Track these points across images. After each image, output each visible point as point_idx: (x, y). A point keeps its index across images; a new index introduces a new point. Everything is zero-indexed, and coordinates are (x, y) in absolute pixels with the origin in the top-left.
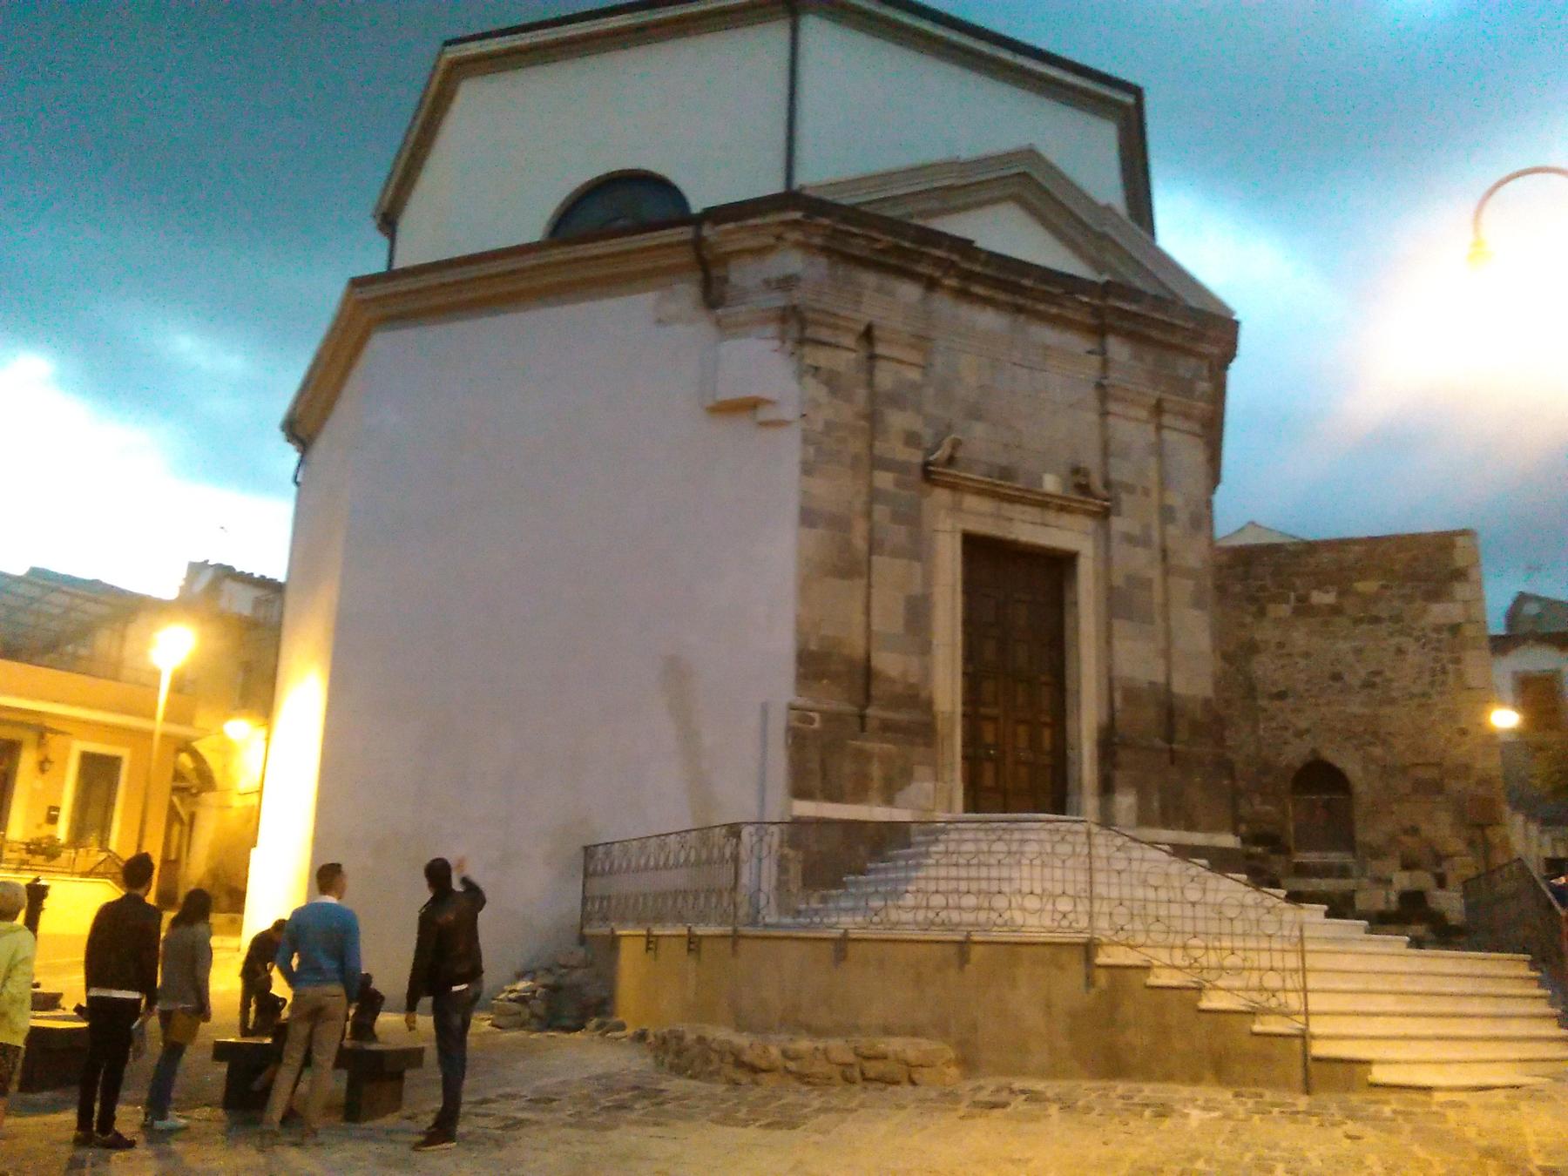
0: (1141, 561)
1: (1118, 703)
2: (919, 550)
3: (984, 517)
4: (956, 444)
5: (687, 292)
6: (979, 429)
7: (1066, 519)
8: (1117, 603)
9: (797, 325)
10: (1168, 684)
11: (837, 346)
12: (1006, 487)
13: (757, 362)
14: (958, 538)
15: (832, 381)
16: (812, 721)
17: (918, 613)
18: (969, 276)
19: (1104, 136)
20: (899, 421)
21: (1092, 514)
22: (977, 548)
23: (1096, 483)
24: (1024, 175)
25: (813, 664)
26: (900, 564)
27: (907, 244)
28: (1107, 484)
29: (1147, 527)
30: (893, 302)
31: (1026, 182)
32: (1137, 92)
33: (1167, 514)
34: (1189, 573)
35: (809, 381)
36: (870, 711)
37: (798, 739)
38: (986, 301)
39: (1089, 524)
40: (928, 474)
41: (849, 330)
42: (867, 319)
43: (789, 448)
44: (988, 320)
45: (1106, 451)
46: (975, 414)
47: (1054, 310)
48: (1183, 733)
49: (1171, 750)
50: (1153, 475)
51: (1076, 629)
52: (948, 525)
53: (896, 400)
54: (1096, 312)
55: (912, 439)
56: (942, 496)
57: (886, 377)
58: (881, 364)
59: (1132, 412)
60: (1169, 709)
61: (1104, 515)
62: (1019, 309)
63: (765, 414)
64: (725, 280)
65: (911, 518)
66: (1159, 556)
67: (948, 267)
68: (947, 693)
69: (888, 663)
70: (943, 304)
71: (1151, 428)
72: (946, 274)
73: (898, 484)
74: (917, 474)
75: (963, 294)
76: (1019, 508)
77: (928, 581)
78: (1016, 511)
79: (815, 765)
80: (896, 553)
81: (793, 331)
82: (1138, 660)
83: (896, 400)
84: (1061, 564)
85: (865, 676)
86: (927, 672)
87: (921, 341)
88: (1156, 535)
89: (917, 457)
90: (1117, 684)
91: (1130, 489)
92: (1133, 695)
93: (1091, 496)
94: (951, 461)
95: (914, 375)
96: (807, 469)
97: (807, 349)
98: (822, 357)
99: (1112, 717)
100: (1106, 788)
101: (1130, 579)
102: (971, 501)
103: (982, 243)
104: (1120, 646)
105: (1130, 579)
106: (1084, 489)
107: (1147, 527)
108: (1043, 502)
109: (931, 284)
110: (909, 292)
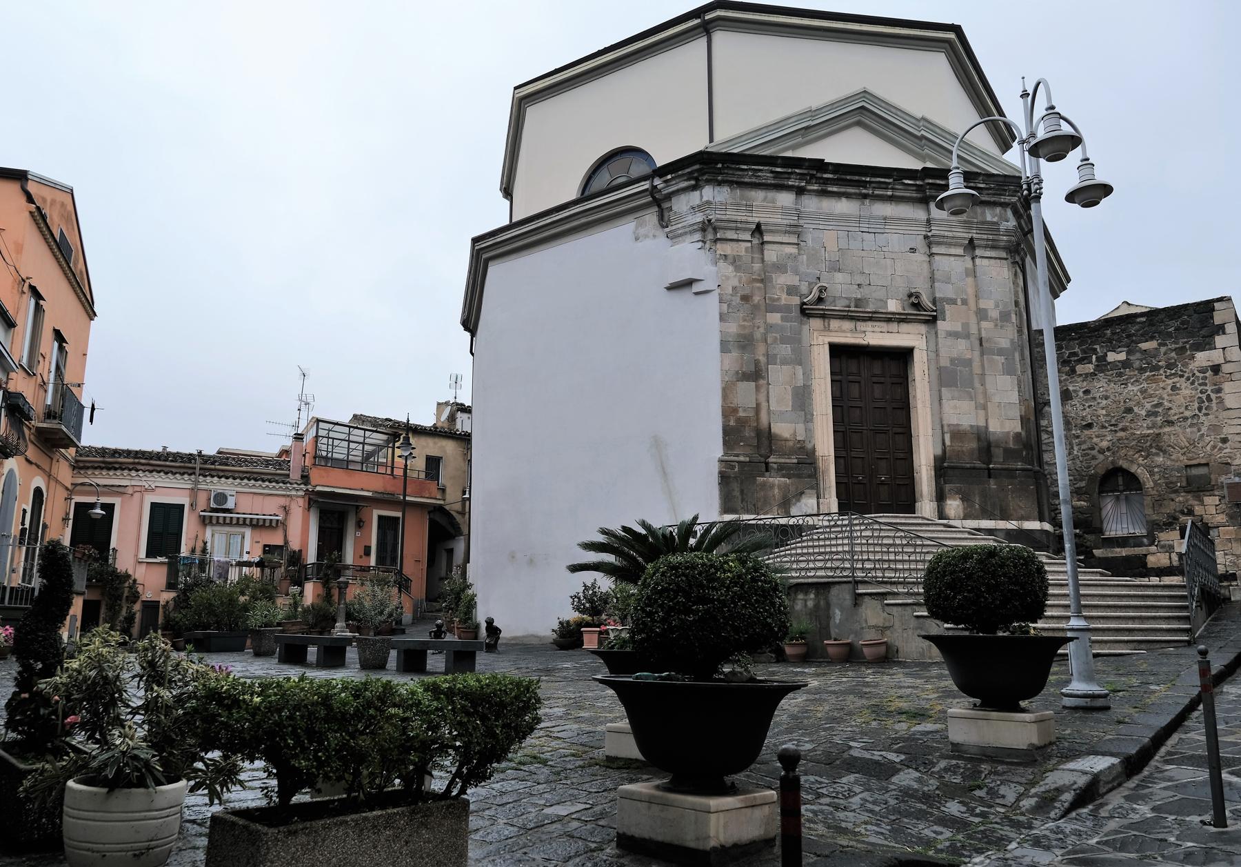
0: (961, 348)
1: (948, 443)
2: (800, 358)
3: (846, 334)
4: (822, 290)
5: (651, 217)
6: (839, 277)
7: (905, 327)
8: (946, 378)
9: (710, 230)
10: (987, 427)
11: (738, 241)
12: (857, 314)
13: (689, 257)
14: (827, 347)
15: (735, 261)
16: (733, 467)
17: (802, 398)
18: (827, 181)
19: (937, 65)
20: (782, 280)
21: (926, 322)
22: (837, 351)
23: (926, 300)
24: (863, 107)
25: (731, 435)
26: (786, 368)
27: (779, 170)
28: (934, 302)
29: (966, 325)
30: (774, 206)
31: (863, 113)
32: (957, 29)
33: (982, 314)
34: (1001, 352)
35: (721, 264)
36: (771, 459)
37: (724, 479)
38: (839, 195)
39: (923, 328)
40: (805, 312)
41: (745, 230)
42: (757, 220)
43: (712, 305)
44: (843, 207)
45: (932, 279)
46: (836, 268)
47: (889, 193)
48: (998, 454)
49: (989, 469)
50: (971, 291)
51: (915, 397)
52: (819, 342)
53: (780, 268)
54: (919, 189)
55: (791, 290)
56: (816, 323)
57: (771, 254)
58: (766, 247)
59: (953, 251)
60: (986, 445)
61: (932, 321)
62: (865, 196)
63: (697, 288)
64: (670, 209)
65: (795, 340)
66: (977, 342)
67: (812, 179)
68: (824, 444)
69: (782, 429)
70: (811, 204)
71: (968, 259)
72: (808, 183)
73: (783, 319)
74: (796, 313)
75: (824, 193)
76: (870, 323)
77: (808, 375)
78: (868, 326)
79: (737, 493)
80: (784, 362)
81: (710, 236)
82: (962, 414)
83: (780, 268)
84: (904, 356)
85: (766, 439)
86: (809, 431)
87: (795, 230)
88: (974, 330)
89: (796, 301)
90: (946, 429)
91: (953, 302)
92: (958, 434)
93: (923, 312)
94: (820, 300)
95: (792, 250)
96: (722, 318)
97: (719, 245)
98: (727, 249)
99: (944, 451)
100: (940, 497)
101: (952, 360)
102: (835, 324)
103: (829, 159)
104: (948, 406)
105: (952, 360)
106: (917, 306)
107: (966, 325)
108: (890, 318)
109: (800, 191)
110: (786, 199)
